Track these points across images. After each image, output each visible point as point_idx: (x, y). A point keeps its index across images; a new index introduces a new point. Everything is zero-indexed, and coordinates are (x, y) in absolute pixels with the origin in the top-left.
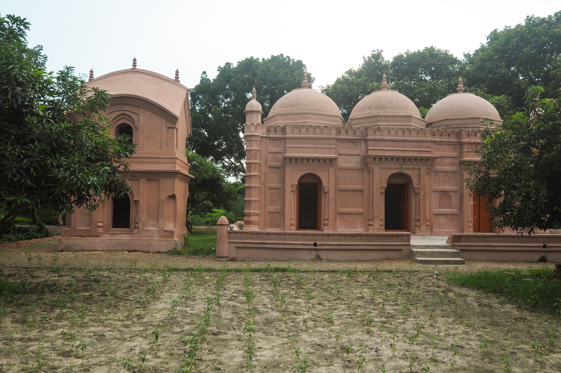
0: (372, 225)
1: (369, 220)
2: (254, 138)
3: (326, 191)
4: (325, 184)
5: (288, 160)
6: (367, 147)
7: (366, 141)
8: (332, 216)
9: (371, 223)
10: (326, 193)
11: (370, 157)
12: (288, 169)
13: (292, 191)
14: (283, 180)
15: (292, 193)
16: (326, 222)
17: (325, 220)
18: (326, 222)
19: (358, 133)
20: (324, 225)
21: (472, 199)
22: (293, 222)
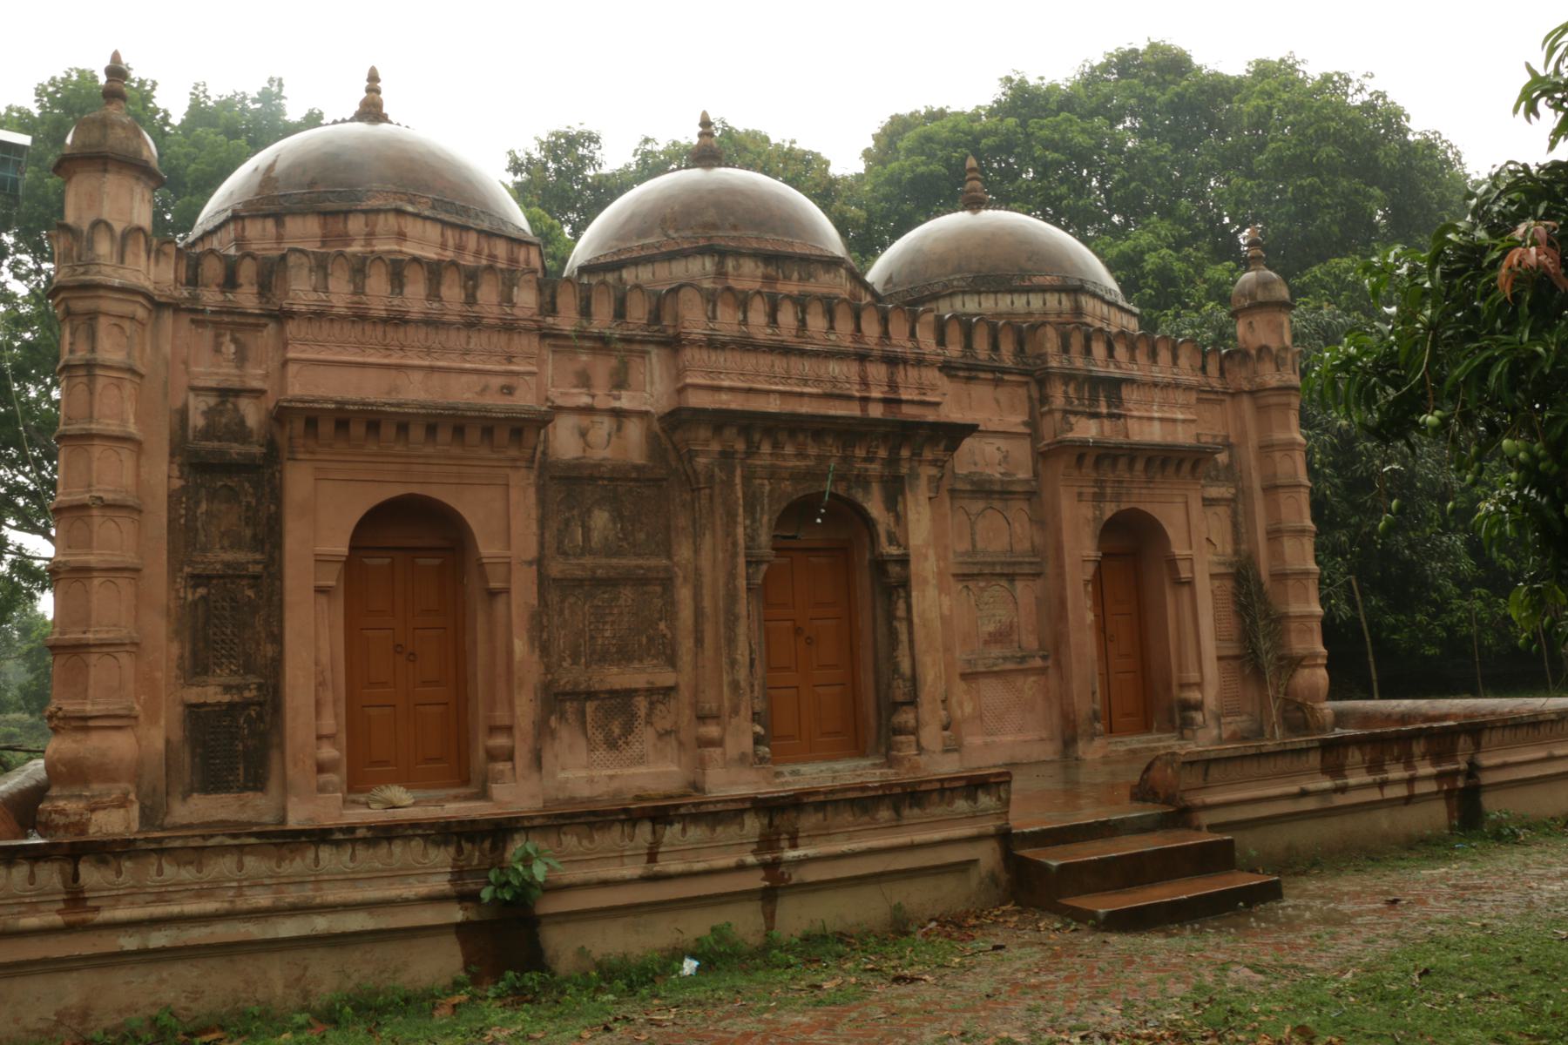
0: (718, 743)
1: (702, 718)
2: (110, 304)
3: (494, 585)
4: (487, 548)
5: (299, 426)
6: (680, 373)
7: (674, 344)
8: (525, 710)
9: (712, 731)
10: (493, 594)
11: (699, 415)
12: (298, 481)
13: (320, 590)
14: (269, 535)
15: (323, 599)
16: (500, 741)
17: (493, 730)
18: (500, 741)
19: (638, 312)
20: (492, 756)
21: (1089, 603)
22: (328, 752)
